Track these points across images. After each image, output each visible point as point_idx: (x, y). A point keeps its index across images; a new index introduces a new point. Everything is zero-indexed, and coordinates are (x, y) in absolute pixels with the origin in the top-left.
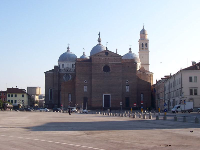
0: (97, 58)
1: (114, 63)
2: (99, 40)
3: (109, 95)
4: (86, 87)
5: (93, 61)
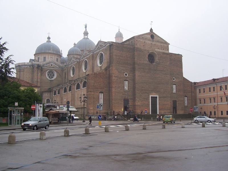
0: (141, 41)
1: (161, 51)
2: (86, 33)
3: (157, 97)
4: (126, 83)
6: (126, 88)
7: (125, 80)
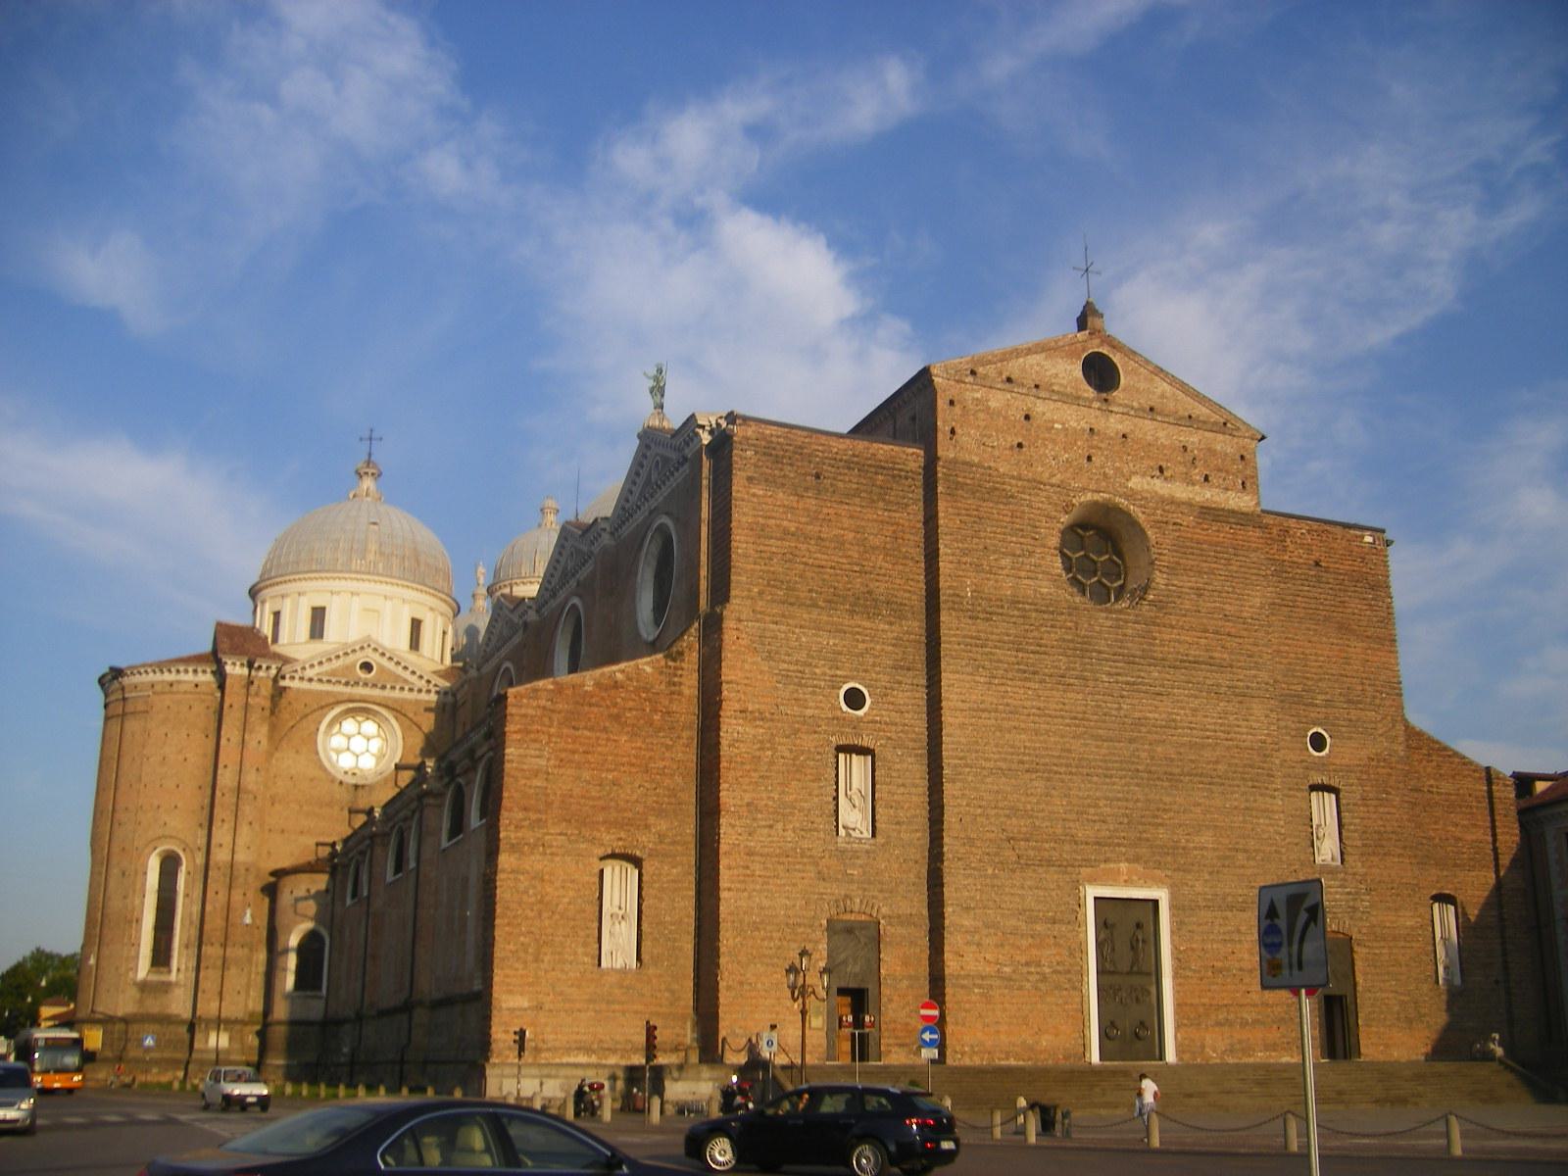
0: (993, 404)
1: (1180, 491)
3: (1156, 902)
5: (953, 431)
6: (854, 818)
7: (840, 749)
